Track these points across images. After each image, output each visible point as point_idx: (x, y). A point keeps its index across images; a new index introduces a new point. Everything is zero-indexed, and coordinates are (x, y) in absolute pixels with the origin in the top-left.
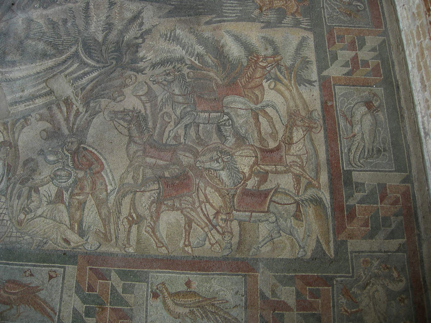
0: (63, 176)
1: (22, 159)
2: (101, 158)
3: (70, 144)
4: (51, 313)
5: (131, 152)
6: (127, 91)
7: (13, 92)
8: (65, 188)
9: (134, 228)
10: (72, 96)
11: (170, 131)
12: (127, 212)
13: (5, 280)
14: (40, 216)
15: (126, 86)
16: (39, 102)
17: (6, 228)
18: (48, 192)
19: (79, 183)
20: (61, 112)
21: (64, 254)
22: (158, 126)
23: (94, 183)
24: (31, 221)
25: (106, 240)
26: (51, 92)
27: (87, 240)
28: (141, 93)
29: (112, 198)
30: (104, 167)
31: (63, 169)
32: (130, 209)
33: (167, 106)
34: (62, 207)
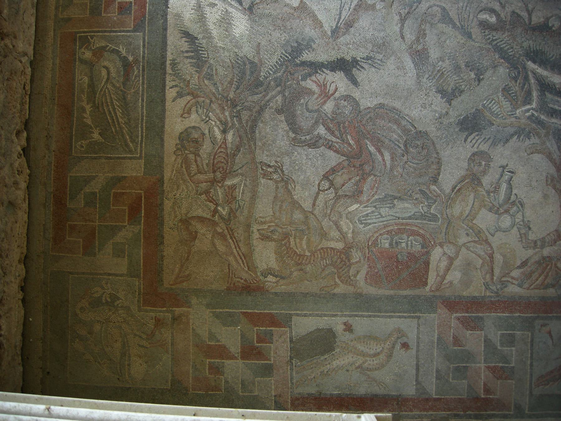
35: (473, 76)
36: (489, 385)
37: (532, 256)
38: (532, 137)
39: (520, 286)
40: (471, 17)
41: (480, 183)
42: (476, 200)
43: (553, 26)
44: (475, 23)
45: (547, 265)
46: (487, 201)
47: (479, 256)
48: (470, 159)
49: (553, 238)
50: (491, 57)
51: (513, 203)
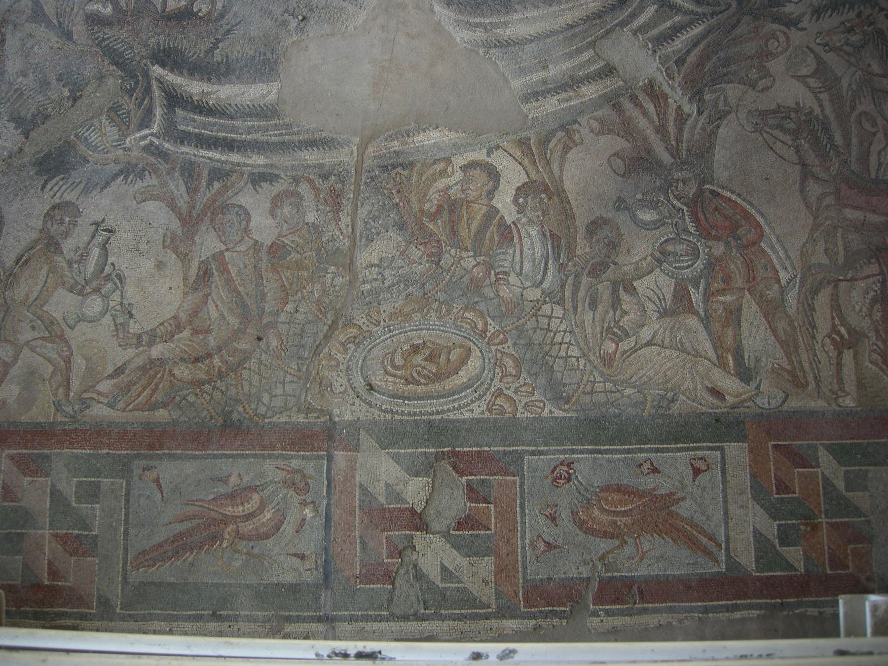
0: (681, 255)
1: (582, 221)
2: (753, 211)
3: (681, 184)
4: (710, 545)
5: (813, 200)
6: (776, 66)
7: (522, 72)
8: (690, 281)
9: (848, 356)
10: (661, 78)
11: (879, 153)
12: (829, 325)
13: (598, 487)
14: (649, 343)
15: (771, 55)
16: (590, 91)
17: (578, 373)
18: (656, 289)
19: (717, 268)
20: (645, 113)
21: (717, 421)
22: (855, 141)
23: (749, 266)
24: (631, 354)
25: (797, 385)
26: (609, 71)
27: (758, 388)
28: (804, 71)
29: (792, 298)
30: (762, 231)
31: (677, 239)
32: (833, 318)
33: (862, 99)
34: (692, 321)
35: (66, 93)
36: (56, 564)
37: (133, 358)
38: (147, 177)
39: (111, 406)
40: (75, 10)
41: (59, 250)
42: (51, 275)
43: (200, 10)
44: (79, 19)
45: (156, 374)
46: (67, 276)
47: (49, 360)
48: (47, 215)
49: (169, 329)
50: (98, 63)
51: (108, 278)
